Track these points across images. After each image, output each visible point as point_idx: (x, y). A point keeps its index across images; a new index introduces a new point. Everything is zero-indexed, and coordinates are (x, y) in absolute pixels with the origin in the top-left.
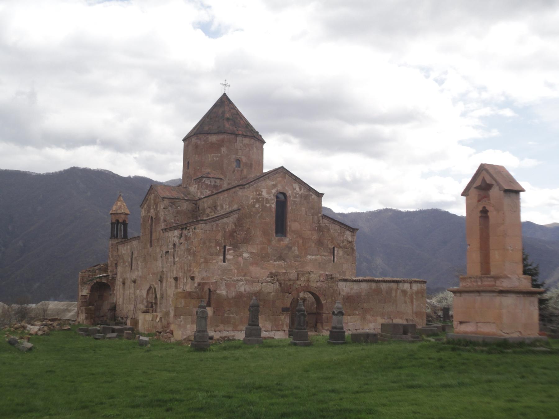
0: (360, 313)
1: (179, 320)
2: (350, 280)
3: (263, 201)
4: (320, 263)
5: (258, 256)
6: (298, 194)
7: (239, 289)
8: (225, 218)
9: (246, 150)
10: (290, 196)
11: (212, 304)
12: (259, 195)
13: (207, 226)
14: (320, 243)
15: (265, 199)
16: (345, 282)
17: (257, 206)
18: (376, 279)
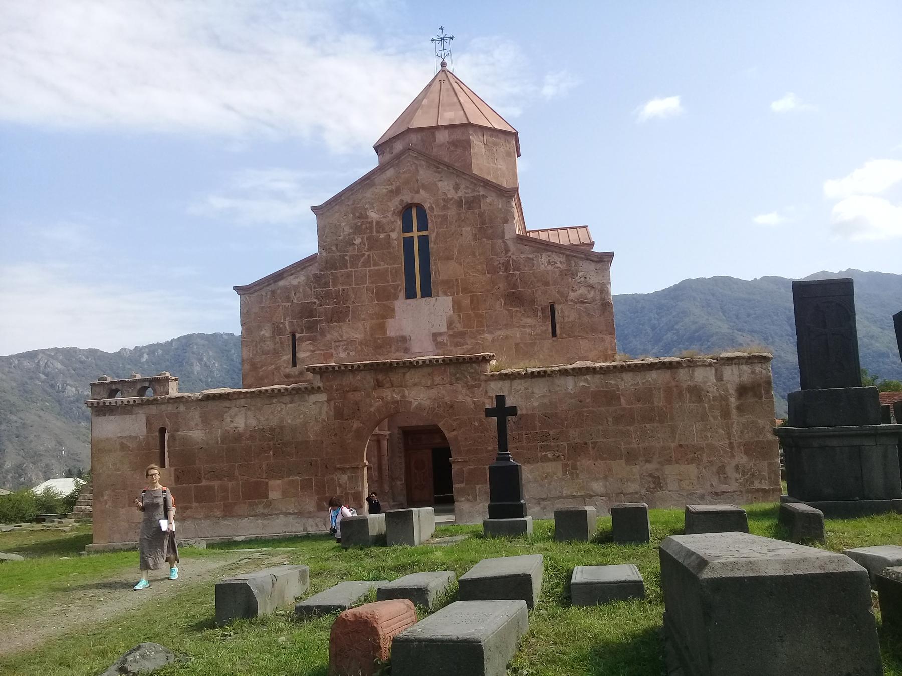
0: (559, 456)
1: (102, 499)
2: (519, 373)
3: (371, 228)
4: (517, 344)
5: (367, 346)
6: (453, 198)
7: (232, 421)
8: (289, 276)
9: (456, 151)
10: (432, 208)
13: (251, 298)
14: (515, 299)
15: (374, 223)
16: (505, 381)
17: (358, 241)
18: (598, 364)
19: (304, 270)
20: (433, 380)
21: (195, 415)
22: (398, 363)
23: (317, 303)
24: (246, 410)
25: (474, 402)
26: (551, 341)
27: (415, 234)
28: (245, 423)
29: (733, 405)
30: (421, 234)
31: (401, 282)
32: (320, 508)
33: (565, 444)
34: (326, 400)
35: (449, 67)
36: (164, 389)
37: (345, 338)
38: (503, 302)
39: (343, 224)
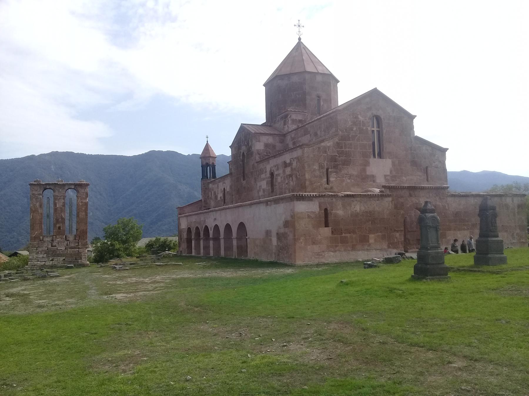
1: (299, 241)
4: (415, 182)
7: (355, 207)
8: (326, 141)
11: (330, 224)
12: (356, 118)
15: (361, 122)
16: (453, 198)
17: (355, 129)
19: (332, 139)
20: (429, 196)
21: (339, 203)
22: (419, 187)
23: (338, 155)
24: (360, 202)
25: (442, 205)
26: (427, 182)
27: (375, 129)
28: (360, 209)
29: (517, 212)
30: (378, 129)
31: (371, 150)
32: (389, 247)
33: (470, 223)
34: (391, 200)
35: (301, 41)
36: (84, 190)
37: (350, 173)
38: (410, 164)
39: (349, 120)
